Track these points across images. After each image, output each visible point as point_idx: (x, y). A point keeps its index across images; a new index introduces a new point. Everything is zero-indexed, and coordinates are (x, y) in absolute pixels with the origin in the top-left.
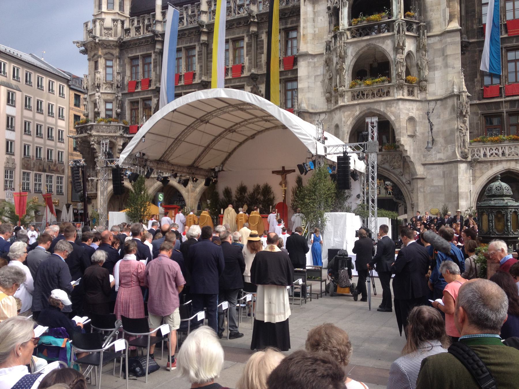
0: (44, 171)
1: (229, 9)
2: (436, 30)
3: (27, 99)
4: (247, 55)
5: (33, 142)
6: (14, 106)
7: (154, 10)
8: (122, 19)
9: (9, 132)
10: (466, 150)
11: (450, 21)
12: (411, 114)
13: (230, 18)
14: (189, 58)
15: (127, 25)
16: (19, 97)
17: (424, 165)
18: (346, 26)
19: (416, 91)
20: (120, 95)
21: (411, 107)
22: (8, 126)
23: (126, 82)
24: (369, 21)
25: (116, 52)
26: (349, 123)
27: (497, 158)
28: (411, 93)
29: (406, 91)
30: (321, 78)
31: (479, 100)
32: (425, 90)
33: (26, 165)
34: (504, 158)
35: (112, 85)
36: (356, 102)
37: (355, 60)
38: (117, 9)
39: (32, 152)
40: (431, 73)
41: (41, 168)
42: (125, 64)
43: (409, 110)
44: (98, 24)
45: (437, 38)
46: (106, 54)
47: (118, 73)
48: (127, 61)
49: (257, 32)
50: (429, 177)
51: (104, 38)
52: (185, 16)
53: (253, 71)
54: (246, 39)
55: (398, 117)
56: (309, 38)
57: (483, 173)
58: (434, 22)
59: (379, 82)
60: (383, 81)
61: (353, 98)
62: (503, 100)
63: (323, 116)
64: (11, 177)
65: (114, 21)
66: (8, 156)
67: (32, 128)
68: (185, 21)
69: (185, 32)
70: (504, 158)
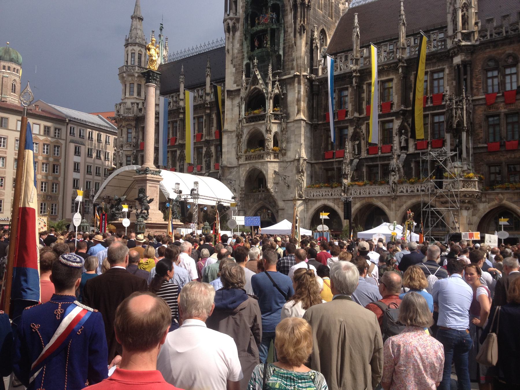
1: (195, 98)
2: (291, 119)
6: (80, 156)
8: (138, 101)
9: (75, 173)
10: (301, 193)
11: (298, 113)
13: (195, 104)
14: (175, 129)
15: (140, 106)
16: (83, 150)
17: (284, 201)
18: (244, 116)
19: (280, 156)
20: (135, 151)
22: (75, 169)
24: (254, 113)
25: (133, 123)
27: (319, 198)
29: (272, 156)
30: (235, 146)
31: (323, 160)
32: (285, 155)
34: (322, 198)
35: (131, 145)
36: (247, 162)
37: (248, 136)
38: (135, 95)
40: (289, 145)
44: (122, 106)
45: (292, 123)
46: (128, 125)
47: (134, 137)
49: (210, 113)
50: (286, 208)
51: (126, 115)
53: (206, 138)
55: (267, 171)
56: (229, 120)
57: (312, 207)
58: (291, 114)
59: (258, 151)
60: (260, 150)
61: (246, 159)
62: (334, 160)
63: (235, 169)
65: (132, 103)
66: (74, 190)
67: (93, 170)
68: (172, 104)
69: (172, 112)
70: (322, 198)
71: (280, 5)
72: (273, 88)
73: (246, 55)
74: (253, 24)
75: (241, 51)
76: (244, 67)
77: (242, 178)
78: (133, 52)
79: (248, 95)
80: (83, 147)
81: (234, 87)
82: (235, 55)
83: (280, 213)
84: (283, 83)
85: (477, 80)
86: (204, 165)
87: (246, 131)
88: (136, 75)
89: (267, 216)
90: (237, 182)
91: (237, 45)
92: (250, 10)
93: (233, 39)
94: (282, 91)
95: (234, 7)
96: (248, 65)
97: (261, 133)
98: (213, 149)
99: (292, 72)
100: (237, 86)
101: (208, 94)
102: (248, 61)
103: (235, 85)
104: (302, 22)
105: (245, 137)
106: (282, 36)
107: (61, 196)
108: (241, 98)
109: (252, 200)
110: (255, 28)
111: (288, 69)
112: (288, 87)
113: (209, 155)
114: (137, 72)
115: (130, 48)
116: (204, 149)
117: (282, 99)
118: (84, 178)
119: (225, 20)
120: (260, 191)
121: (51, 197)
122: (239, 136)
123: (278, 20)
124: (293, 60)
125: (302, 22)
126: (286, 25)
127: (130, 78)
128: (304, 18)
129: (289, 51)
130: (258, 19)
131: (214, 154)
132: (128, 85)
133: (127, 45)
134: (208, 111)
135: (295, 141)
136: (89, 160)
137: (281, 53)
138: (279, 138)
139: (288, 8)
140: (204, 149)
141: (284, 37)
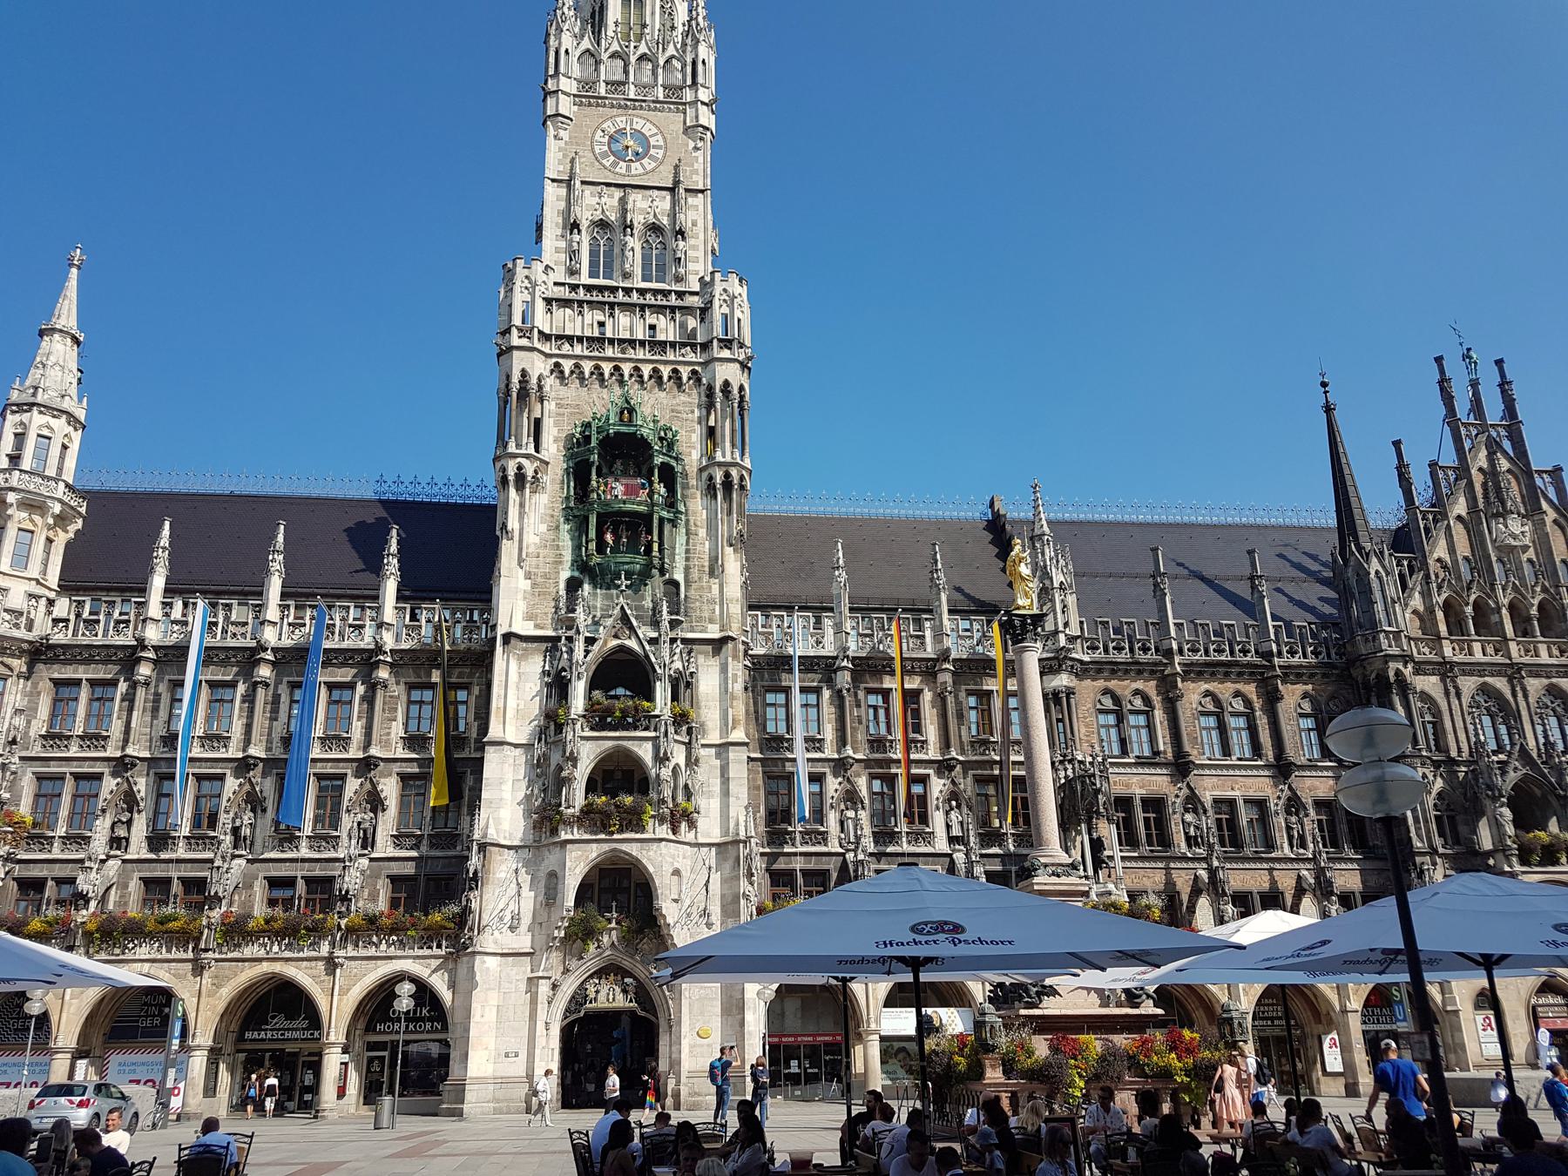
4: (359, 718)
7: (143, 591)
12: (677, 865)
18: (580, 711)
23: (32, 734)
26: (578, 871)
42: (39, 694)
43: (673, 857)
48: (46, 687)
52: (221, 620)
71: (679, 469)
72: (672, 654)
73: (568, 556)
76: (562, 586)
78: (46, 432)
81: (527, 629)
85: (1087, 726)
89: (620, 996)
97: (637, 762)
100: (537, 626)
102: (576, 574)
103: (532, 623)
106: (681, 539)
114: (60, 501)
123: (671, 503)
137: (679, 576)
141: (687, 543)
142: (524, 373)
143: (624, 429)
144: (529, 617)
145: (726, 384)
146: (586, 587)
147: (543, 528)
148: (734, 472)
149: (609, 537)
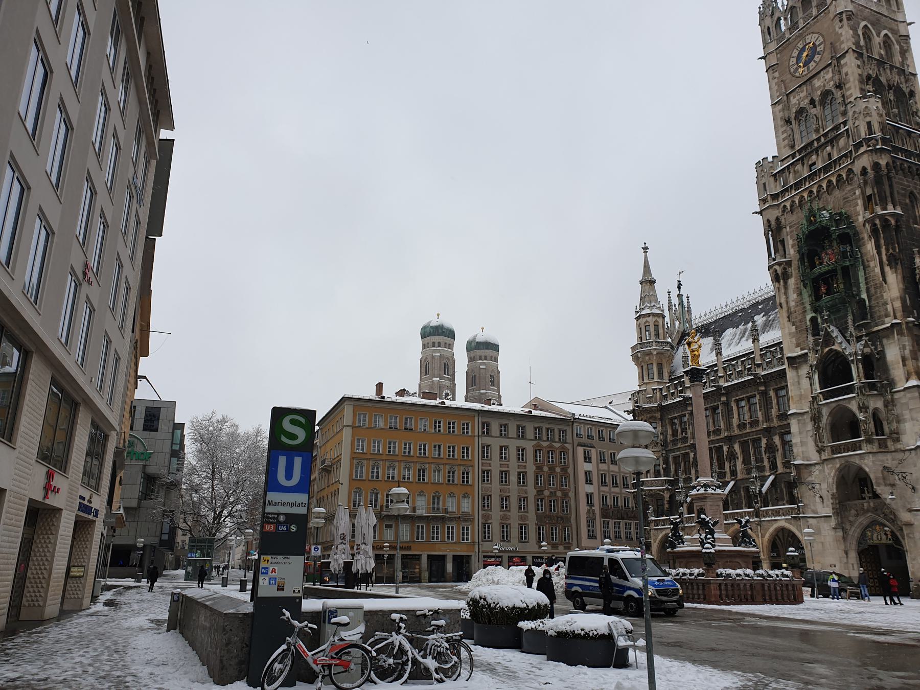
0: (623, 519)
3: (601, 454)
5: (610, 492)
21: (885, 458)
25: (658, 415)
28: (883, 445)
30: (811, 433)
33: (605, 514)
39: (610, 502)
40: (902, 425)
41: (619, 516)
43: (882, 461)
46: (651, 417)
50: (916, 523)
54: (758, 396)
56: (796, 399)
58: (897, 379)
63: (817, 467)
64: (593, 526)
67: (608, 480)
73: (808, 307)
74: (812, 266)
75: (801, 303)
77: (830, 480)
79: (821, 361)
80: (593, 450)
81: (798, 352)
82: (792, 309)
83: (906, 531)
84: (876, 338)
86: (766, 463)
87: (825, 412)
88: (655, 353)
89: (884, 537)
90: (824, 486)
91: (793, 296)
92: (805, 250)
93: (786, 288)
94: (876, 349)
95: (780, 247)
96: (813, 320)
98: (777, 440)
99: (887, 320)
100: (802, 349)
101: (758, 365)
102: (813, 314)
104: (891, 251)
105: (825, 420)
106: (861, 273)
107: (573, 516)
108: (811, 366)
109: (853, 512)
110: (817, 270)
111: (880, 317)
112: (885, 341)
113: (771, 448)
115: (642, 320)
116: (764, 442)
117: (878, 359)
118: (599, 492)
119: (770, 268)
120: (864, 499)
121: (562, 518)
122: (816, 419)
124: (886, 304)
125: (891, 251)
126: (865, 258)
127: (647, 358)
128: (893, 244)
129: (876, 292)
130: (820, 259)
131: (779, 447)
132: (645, 367)
133: (637, 319)
134: (762, 388)
135: (912, 419)
136: (603, 467)
137: (864, 296)
138: (883, 415)
139: (866, 236)
140: (764, 442)
142: (769, 221)
143: (812, 228)
144: (798, 345)
145: (864, 169)
146: (819, 320)
147: (795, 296)
148: (877, 222)
149: (823, 289)
